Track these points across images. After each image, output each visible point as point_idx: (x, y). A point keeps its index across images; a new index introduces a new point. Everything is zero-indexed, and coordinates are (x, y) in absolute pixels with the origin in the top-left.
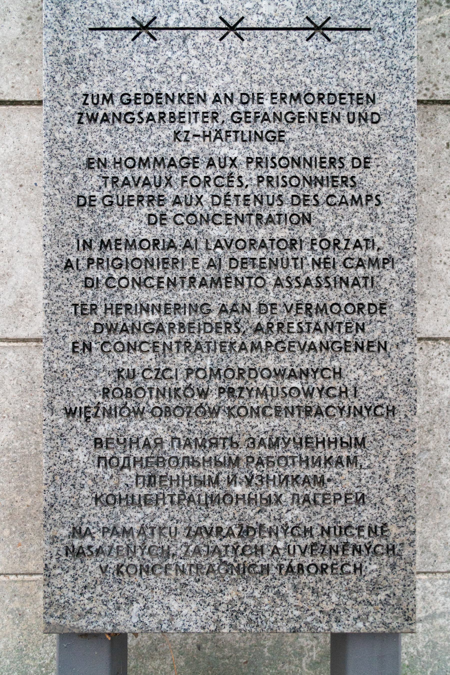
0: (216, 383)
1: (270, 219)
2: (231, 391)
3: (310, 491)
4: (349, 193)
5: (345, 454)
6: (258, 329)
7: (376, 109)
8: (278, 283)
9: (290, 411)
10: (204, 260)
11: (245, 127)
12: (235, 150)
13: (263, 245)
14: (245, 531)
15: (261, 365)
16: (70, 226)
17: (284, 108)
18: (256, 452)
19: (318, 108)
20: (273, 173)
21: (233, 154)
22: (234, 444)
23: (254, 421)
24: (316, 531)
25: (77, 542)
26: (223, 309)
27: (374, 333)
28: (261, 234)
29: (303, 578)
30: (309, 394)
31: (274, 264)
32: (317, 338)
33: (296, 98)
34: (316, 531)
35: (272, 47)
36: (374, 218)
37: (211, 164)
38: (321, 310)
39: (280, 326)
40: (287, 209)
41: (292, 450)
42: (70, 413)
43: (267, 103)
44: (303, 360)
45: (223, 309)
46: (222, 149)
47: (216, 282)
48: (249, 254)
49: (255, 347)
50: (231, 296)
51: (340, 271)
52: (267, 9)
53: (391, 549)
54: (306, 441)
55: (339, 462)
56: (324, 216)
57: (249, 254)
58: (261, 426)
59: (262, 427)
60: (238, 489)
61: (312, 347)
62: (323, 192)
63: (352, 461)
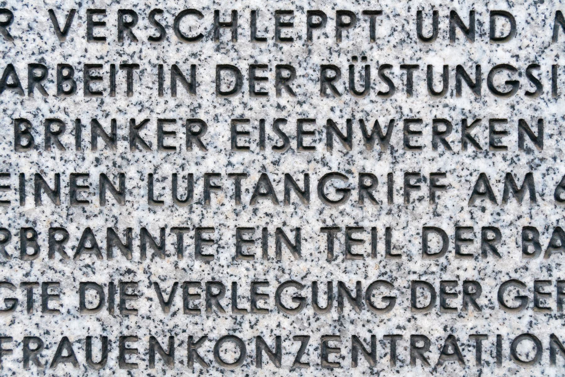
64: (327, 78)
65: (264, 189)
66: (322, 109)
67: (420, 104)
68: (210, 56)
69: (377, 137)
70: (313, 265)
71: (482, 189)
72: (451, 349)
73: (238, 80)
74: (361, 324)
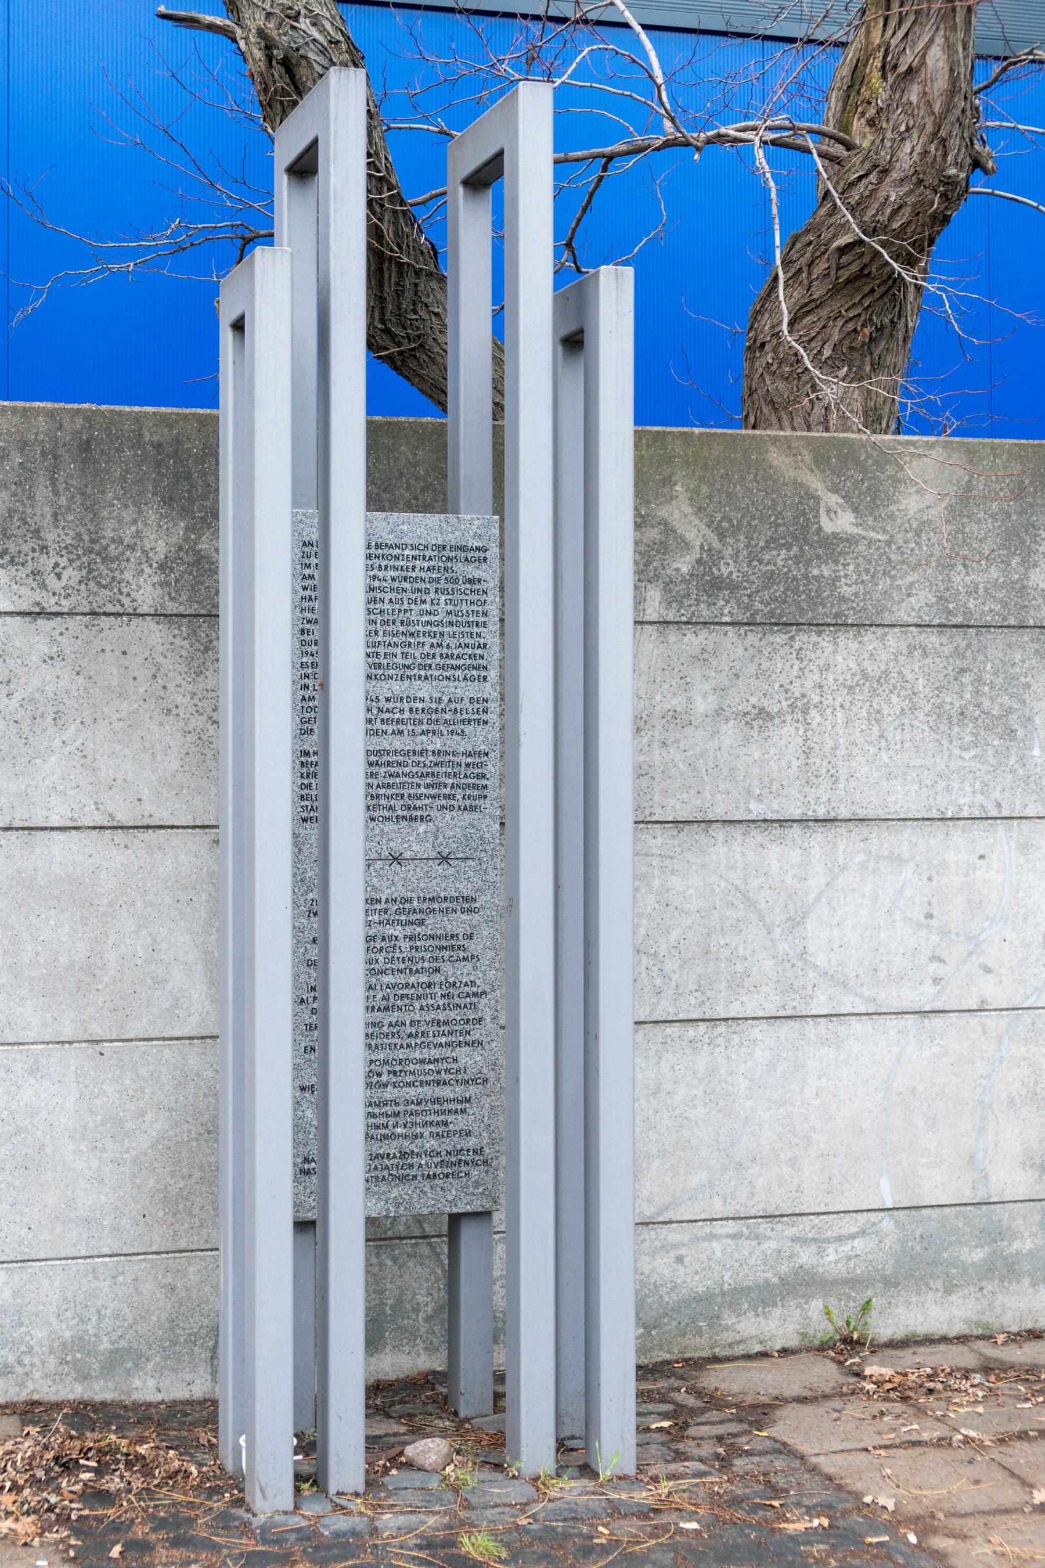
0: (386, 1067)
1: (417, 971)
2: (395, 1073)
3: (440, 1130)
4: (462, 954)
5: (459, 1107)
6: (410, 1036)
7: (477, 905)
8: (422, 1008)
9: (428, 1083)
10: (380, 996)
11: (403, 918)
12: (397, 931)
13: (413, 986)
14: (403, 1155)
15: (411, 1057)
16: (303, 978)
17: (425, 906)
18: (409, 1108)
19: (444, 905)
20: (418, 944)
21: (396, 933)
22: (397, 1104)
23: (408, 1090)
24: (444, 1153)
25: (306, 1166)
26: (390, 1025)
27: (475, 1036)
28: (412, 980)
29: (436, 1181)
30: (439, 1072)
31: (419, 997)
32: (444, 1040)
33: (432, 899)
34: (444, 1153)
35: (418, 870)
36: (475, 969)
37: (384, 939)
38: (446, 1023)
39: (423, 1033)
40: (426, 965)
41: (430, 1106)
42: (303, 1089)
43: (415, 903)
44: (436, 1053)
45: (390, 1025)
46: (390, 931)
47: (386, 1009)
48: (405, 992)
49: (409, 1046)
50: (394, 1017)
51: (457, 1000)
52: (416, 847)
53: (485, 1162)
54: (438, 1101)
55: (456, 1112)
56: (447, 968)
57: (405, 992)
58: (412, 1092)
59: (413, 1093)
60: (399, 1130)
61: (441, 1045)
62: (446, 954)
63: (463, 1111)
64: (402, 623)
65: (390, 644)
66: (401, 629)
67: (420, 628)
68: (379, 618)
69: (412, 635)
70: (399, 660)
71: (432, 645)
72: (426, 678)
73: (385, 623)
74: (409, 672)
